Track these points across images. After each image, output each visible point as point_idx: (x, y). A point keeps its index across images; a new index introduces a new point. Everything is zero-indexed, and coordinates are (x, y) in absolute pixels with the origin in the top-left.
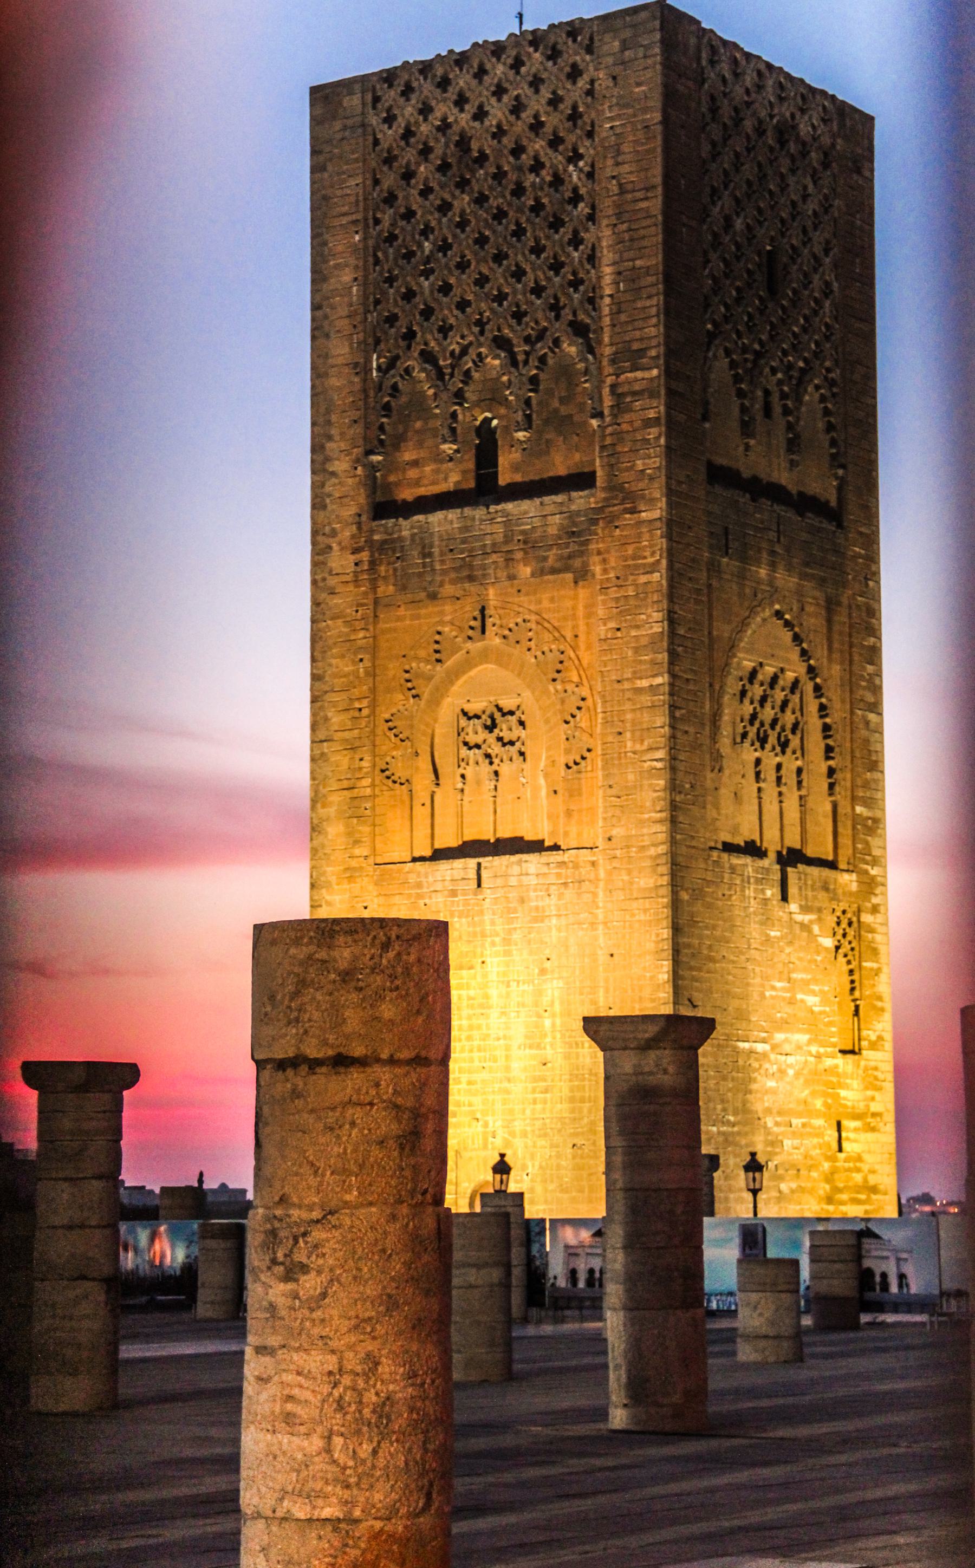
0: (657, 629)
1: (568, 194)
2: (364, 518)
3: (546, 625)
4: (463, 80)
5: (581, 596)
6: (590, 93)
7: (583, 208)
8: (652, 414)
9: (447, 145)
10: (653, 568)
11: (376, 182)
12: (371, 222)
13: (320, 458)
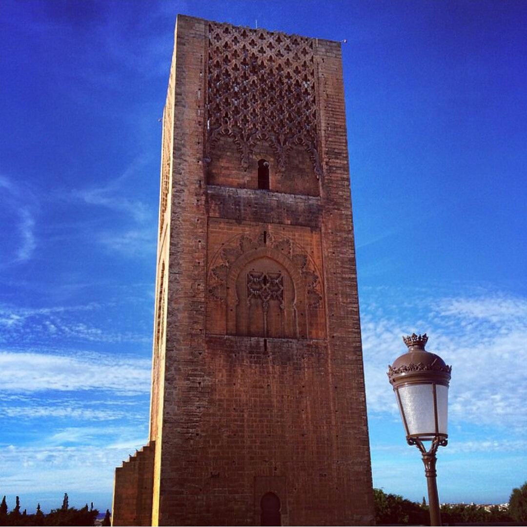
3: (298, 245)
5: (314, 237)
6: (312, 60)
7: (310, 98)
9: (246, 56)
11: (210, 58)
12: (208, 71)
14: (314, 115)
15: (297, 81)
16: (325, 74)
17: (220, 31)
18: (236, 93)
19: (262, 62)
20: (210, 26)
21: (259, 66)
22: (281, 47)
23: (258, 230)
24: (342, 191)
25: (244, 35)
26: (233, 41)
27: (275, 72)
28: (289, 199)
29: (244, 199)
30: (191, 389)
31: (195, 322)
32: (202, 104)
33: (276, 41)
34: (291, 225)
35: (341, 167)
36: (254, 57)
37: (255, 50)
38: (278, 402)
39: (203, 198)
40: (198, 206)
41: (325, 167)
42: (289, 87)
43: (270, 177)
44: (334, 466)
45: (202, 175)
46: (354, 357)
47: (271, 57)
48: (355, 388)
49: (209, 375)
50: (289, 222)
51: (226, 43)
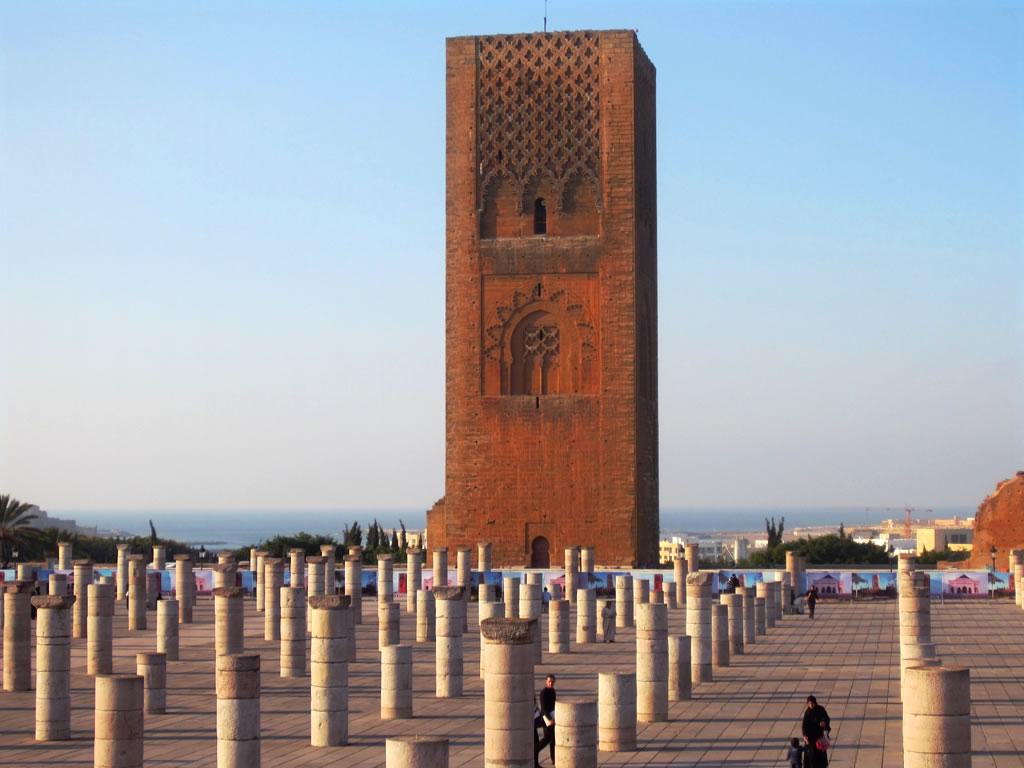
0: (631, 301)
1: (585, 106)
2: (475, 238)
4: (528, 46)
6: (597, 63)
7: (593, 113)
8: (629, 207)
10: (628, 273)
13: (451, 208)
14: (597, 135)
15: (579, 94)
16: (612, 80)
17: (491, 48)
18: (510, 124)
19: (539, 78)
20: (481, 43)
21: (536, 83)
22: (561, 53)
23: (533, 283)
24: (625, 226)
25: (519, 46)
26: (507, 57)
27: (554, 87)
28: (564, 243)
29: (518, 250)
30: (469, 447)
31: (471, 385)
32: (473, 145)
33: (556, 45)
34: (566, 273)
35: (623, 197)
36: (530, 73)
37: (530, 64)
38: (549, 456)
39: (477, 254)
40: (471, 265)
41: (606, 199)
42: (569, 104)
43: (547, 219)
44: (600, 514)
45: (475, 229)
46: (626, 411)
47: (549, 68)
48: (625, 441)
49: (485, 434)
50: (564, 270)
51: (500, 61)
